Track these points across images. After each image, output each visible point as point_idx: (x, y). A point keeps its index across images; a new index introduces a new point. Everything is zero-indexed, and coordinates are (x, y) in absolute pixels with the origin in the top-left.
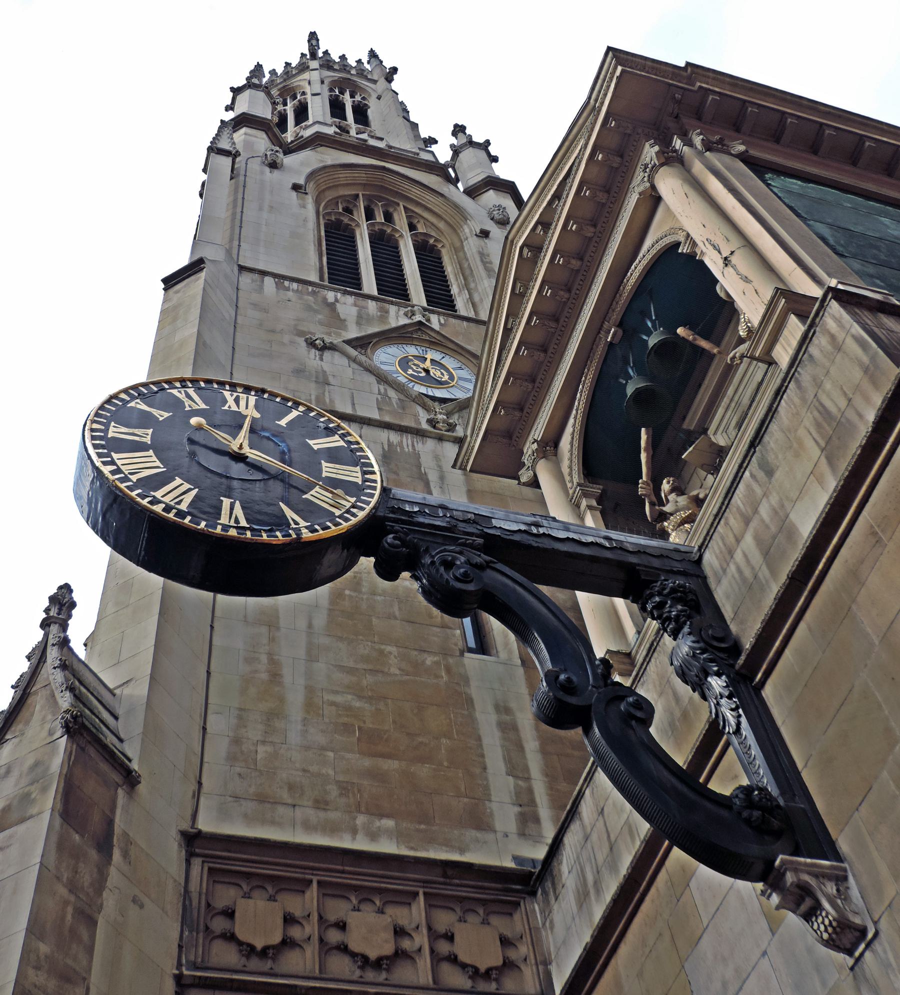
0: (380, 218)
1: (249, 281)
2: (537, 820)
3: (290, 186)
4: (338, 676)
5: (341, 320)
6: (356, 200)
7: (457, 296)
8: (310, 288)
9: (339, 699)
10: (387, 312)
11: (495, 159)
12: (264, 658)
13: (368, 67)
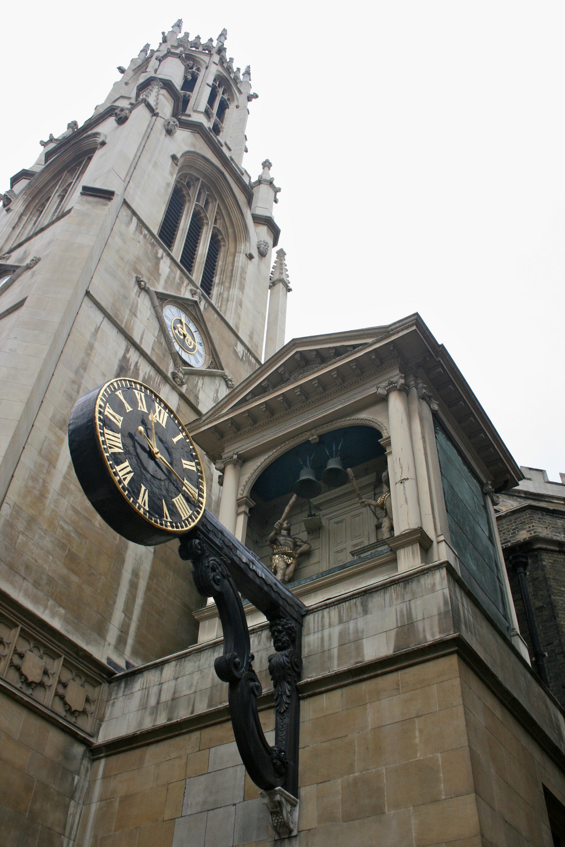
0: (202, 204)
1: (125, 214)
2: (125, 644)
3: (172, 154)
4: (70, 512)
5: (158, 273)
6: (196, 181)
7: (215, 285)
8: (153, 240)
9: (66, 527)
10: (183, 282)
11: (276, 201)
12: (41, 481)
13: (241, 77)
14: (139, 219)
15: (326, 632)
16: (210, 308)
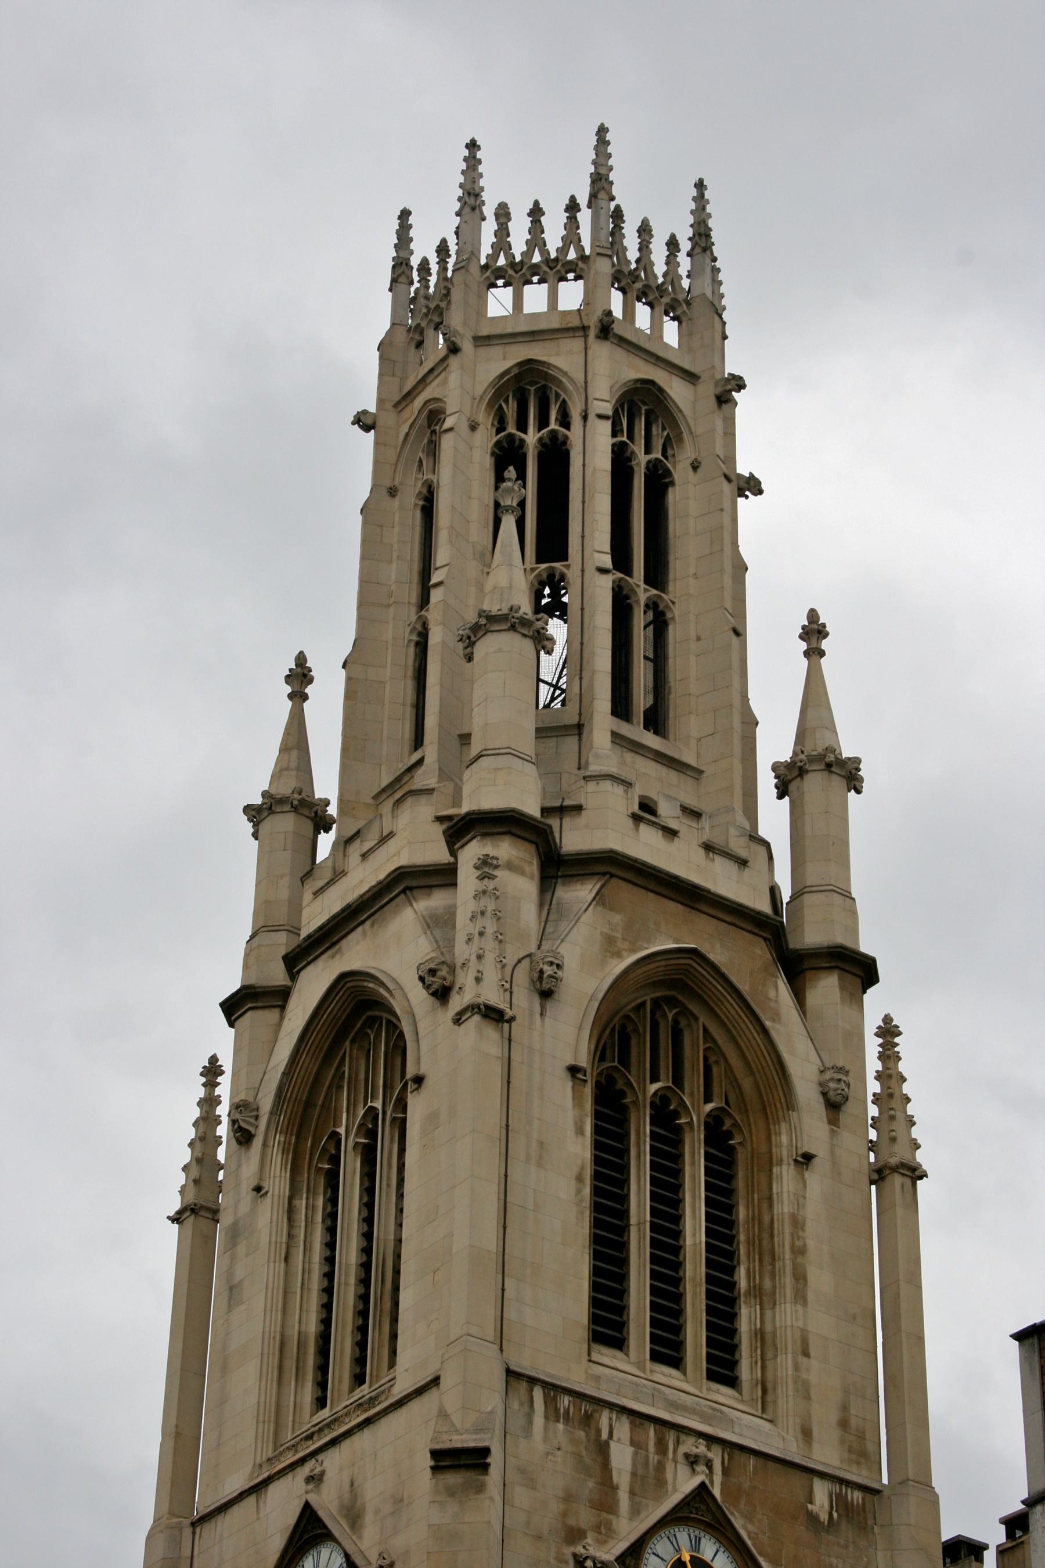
7: (742, 1299)
14: (547, 1385)
16: (737, 1453)
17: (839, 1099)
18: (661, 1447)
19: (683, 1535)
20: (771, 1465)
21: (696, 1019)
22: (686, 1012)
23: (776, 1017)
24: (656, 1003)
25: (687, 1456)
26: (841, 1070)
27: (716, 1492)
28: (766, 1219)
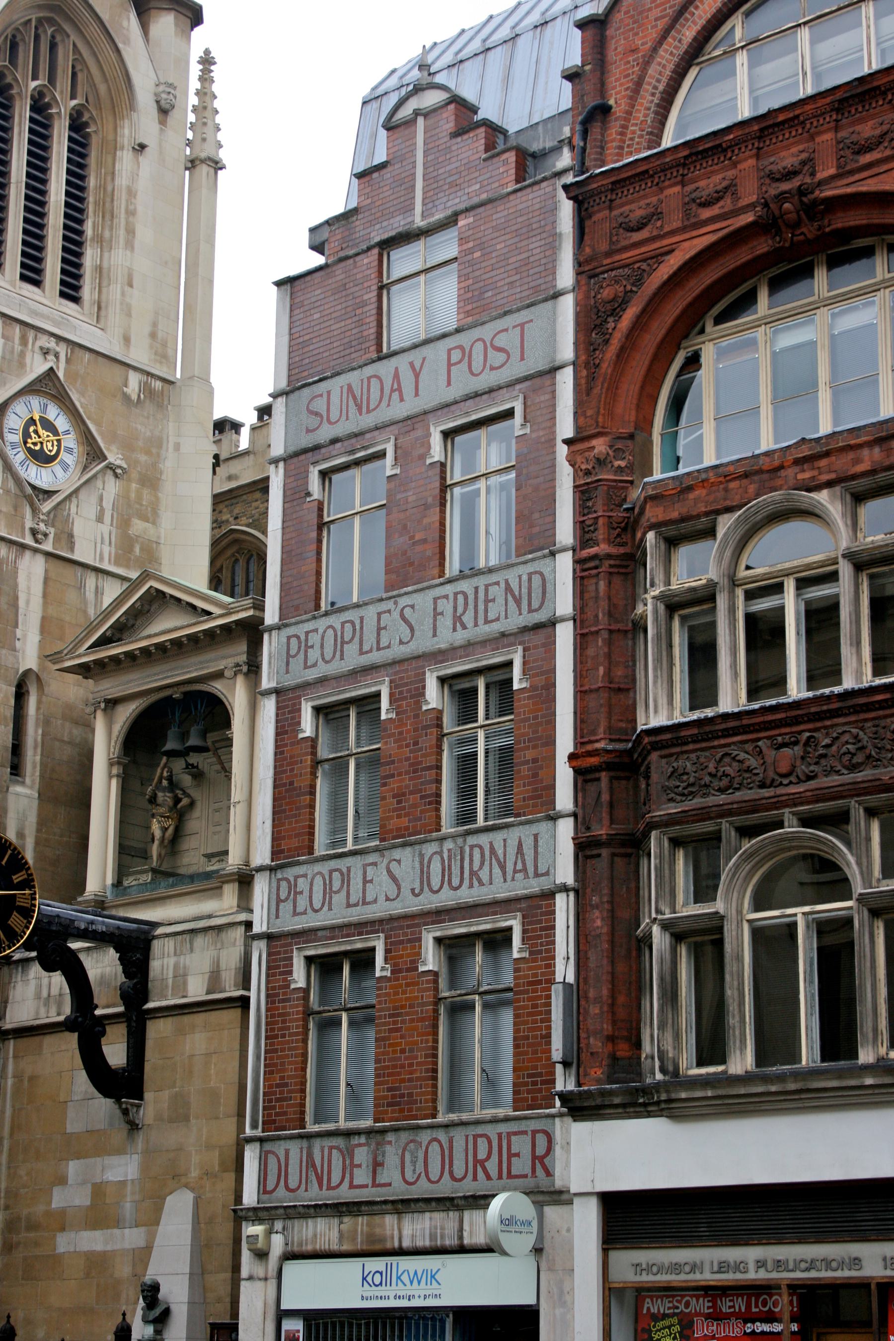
15: (166, 960)
16: (77, 349)
17: (168, 106)
18: (24, 341)
19: (35, 402)
20: (100, 359)
21: (68, 36)
22: (60, 30)
23: (127, 41)
24: (40, 21)
25: (41, 348)
26: (170, 85)
27: (61, 374)
28: (109, 188)
